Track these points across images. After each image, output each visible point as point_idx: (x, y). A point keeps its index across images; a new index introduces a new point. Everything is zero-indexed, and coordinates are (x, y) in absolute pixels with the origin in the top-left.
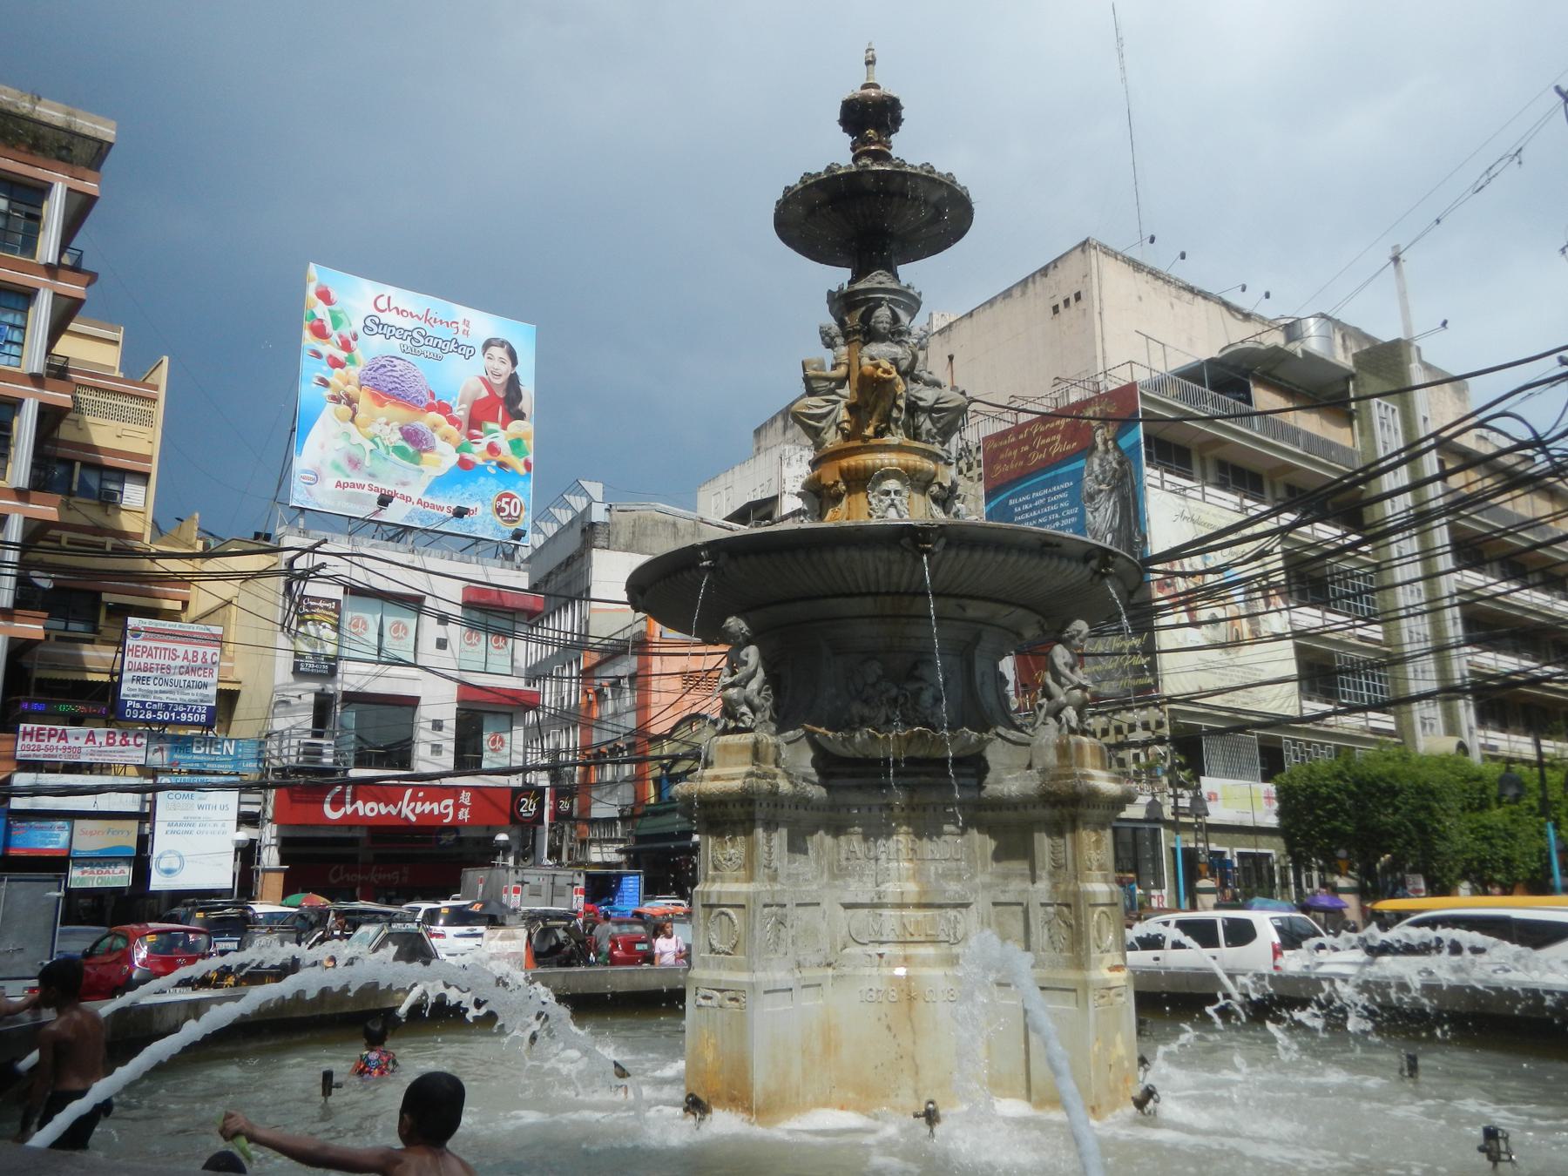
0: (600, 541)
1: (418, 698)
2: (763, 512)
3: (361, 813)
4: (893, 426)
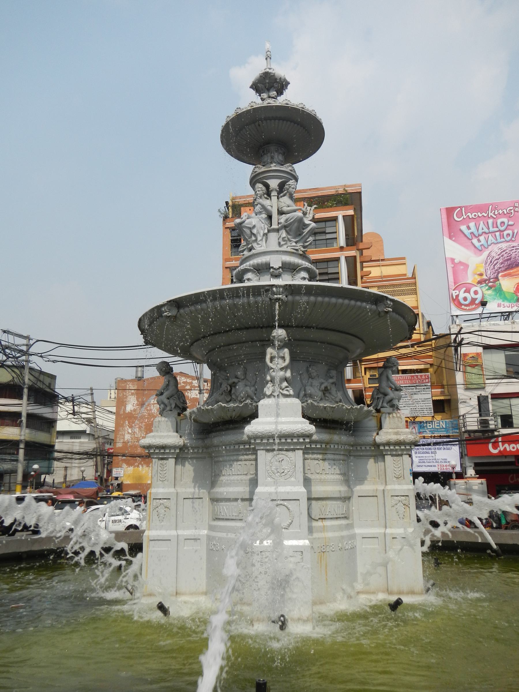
3: (508, 450)
4: (255, 245)
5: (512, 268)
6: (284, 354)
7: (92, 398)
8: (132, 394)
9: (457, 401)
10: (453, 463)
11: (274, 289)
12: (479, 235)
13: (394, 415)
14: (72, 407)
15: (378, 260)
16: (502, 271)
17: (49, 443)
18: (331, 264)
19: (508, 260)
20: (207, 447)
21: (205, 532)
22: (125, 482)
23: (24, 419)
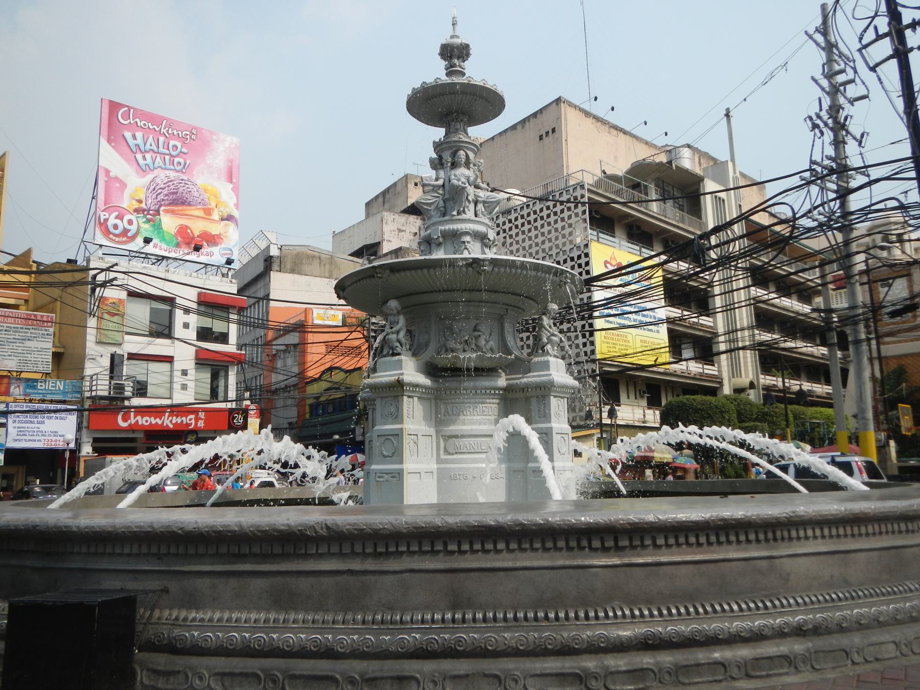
0: (275, 266)
1: (172, 357)
2: (372, 251)
3: (140, 423)
5: (177, 204)
12: (146, 152)
16: (165, 205)
19: (173, 193)
21: (435, 466)
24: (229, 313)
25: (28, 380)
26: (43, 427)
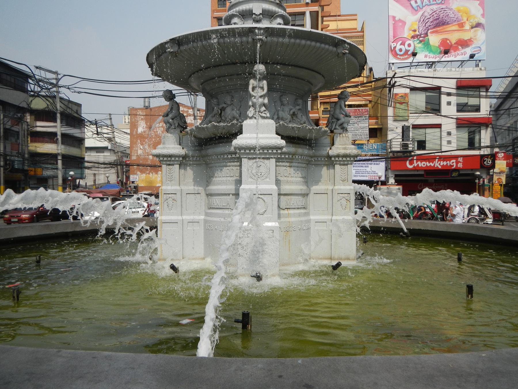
1: (441, 125)
3: (420, 166)
5: (439, 26)
6: (263, 85)
7: (111, 122)
8: (142, 119)
9: (387, 129)
10: (380, 174)
11: (257, 31)
13: (344, 135)
14: (96, 129)
15: (336, 16)
16: (431, 29)
17: (80, 156)
18: (298, 17)
19: (436, 19)
20: (203, 157)
21: (202, 217)
22: (140, 185)
23: (59, 137)
24: (480, 91)
25: (358, 144)
26: (368, 169)
